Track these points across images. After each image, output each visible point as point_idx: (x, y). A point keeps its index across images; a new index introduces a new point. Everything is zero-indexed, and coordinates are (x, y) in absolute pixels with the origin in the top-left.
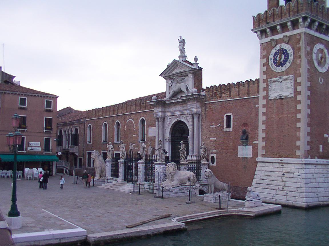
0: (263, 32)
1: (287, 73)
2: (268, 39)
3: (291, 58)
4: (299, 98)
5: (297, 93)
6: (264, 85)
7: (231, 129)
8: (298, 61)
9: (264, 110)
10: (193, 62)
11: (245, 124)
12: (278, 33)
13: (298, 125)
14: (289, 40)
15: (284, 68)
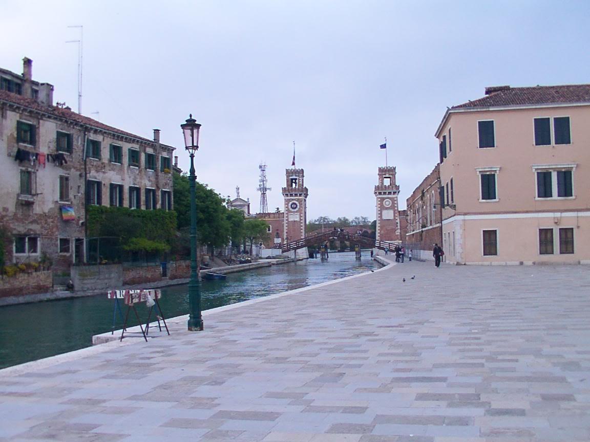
0: (287, 195)
1: (297, 212)
2: (288, 198)
3: (298, 207)
4: (302, 221)
5: (301, 220)
6: (287, 215)
7: (271, 232)
8: (301, 209)
9: (287, 225)
10: (247, 200)
11: (278, 230)
12: (293, 196)
13: (302, 231)
14: (298, 200)
15: (295, 210)
